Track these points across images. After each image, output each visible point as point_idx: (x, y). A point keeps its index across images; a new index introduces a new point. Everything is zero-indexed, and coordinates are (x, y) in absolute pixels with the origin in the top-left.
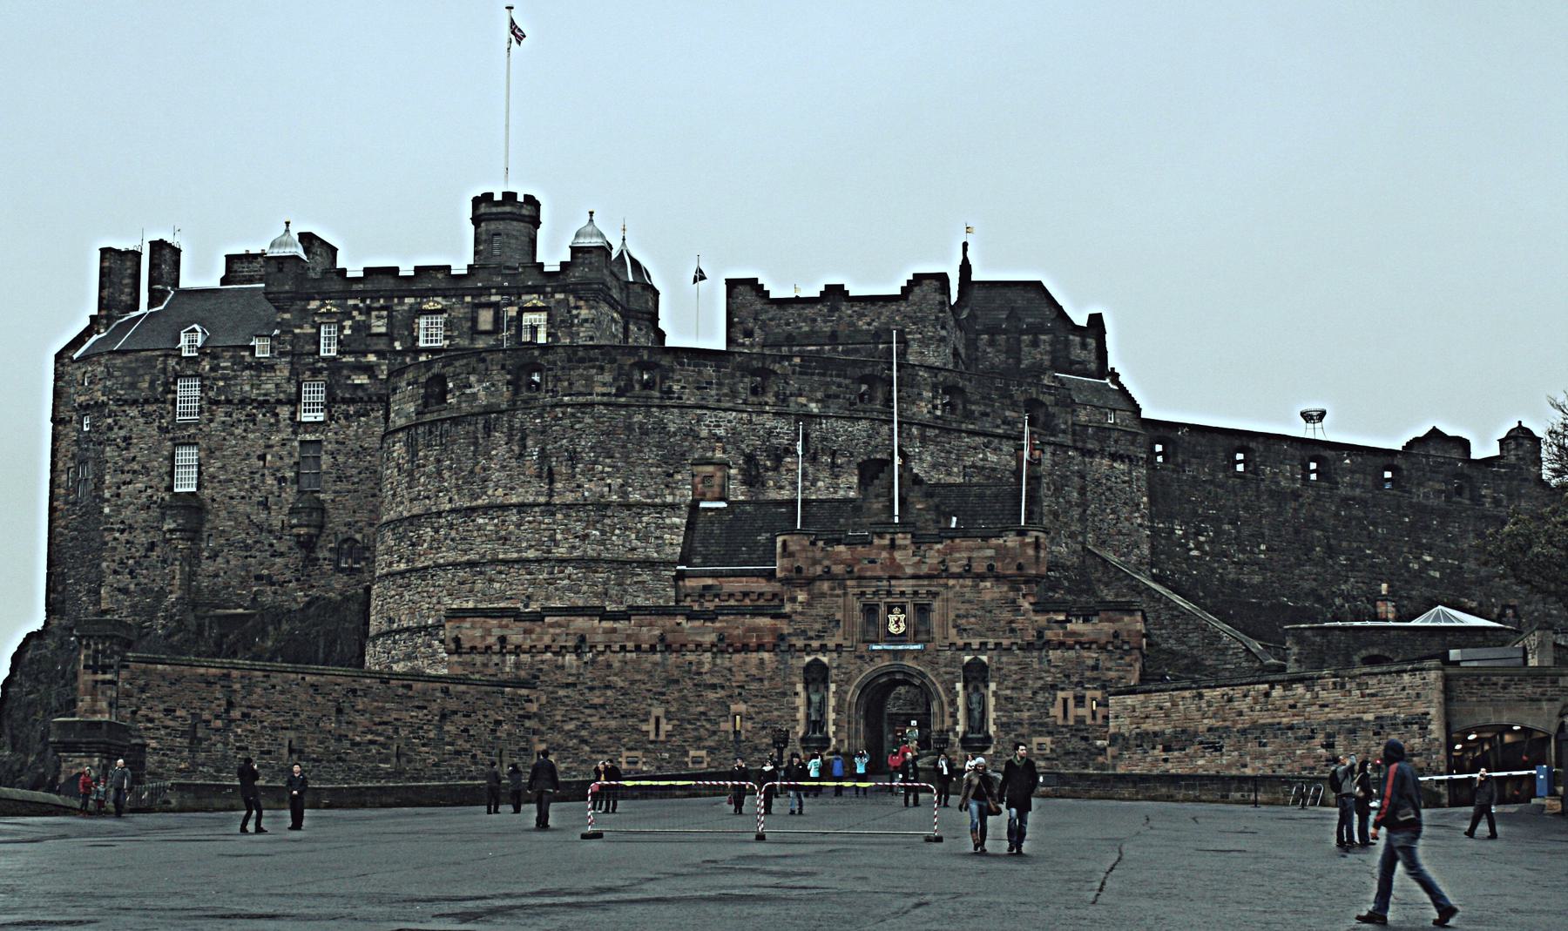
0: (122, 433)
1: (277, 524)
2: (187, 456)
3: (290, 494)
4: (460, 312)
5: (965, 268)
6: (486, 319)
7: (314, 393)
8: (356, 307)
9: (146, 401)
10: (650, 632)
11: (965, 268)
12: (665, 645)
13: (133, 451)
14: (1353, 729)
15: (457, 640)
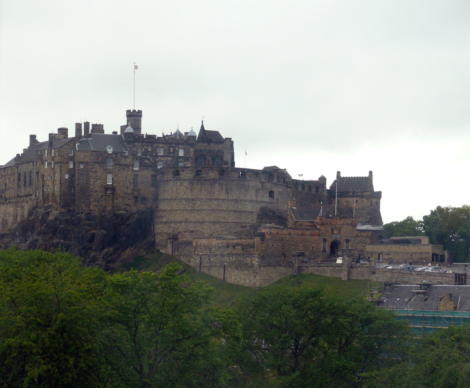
0: (95, 170)
1: (129, 193)
2: (110, 177)
3: (132, 186)
4: (166, 148)
5: (202, 127)
6: (172, 150)
7: (137, 164)
8: (145, 145)
9: (101, 163)
10: (300, 232)
11: (202, 127)
12: (303, 234)
13: (97, 174)
14: (416, 253)
15: (271, 233)
